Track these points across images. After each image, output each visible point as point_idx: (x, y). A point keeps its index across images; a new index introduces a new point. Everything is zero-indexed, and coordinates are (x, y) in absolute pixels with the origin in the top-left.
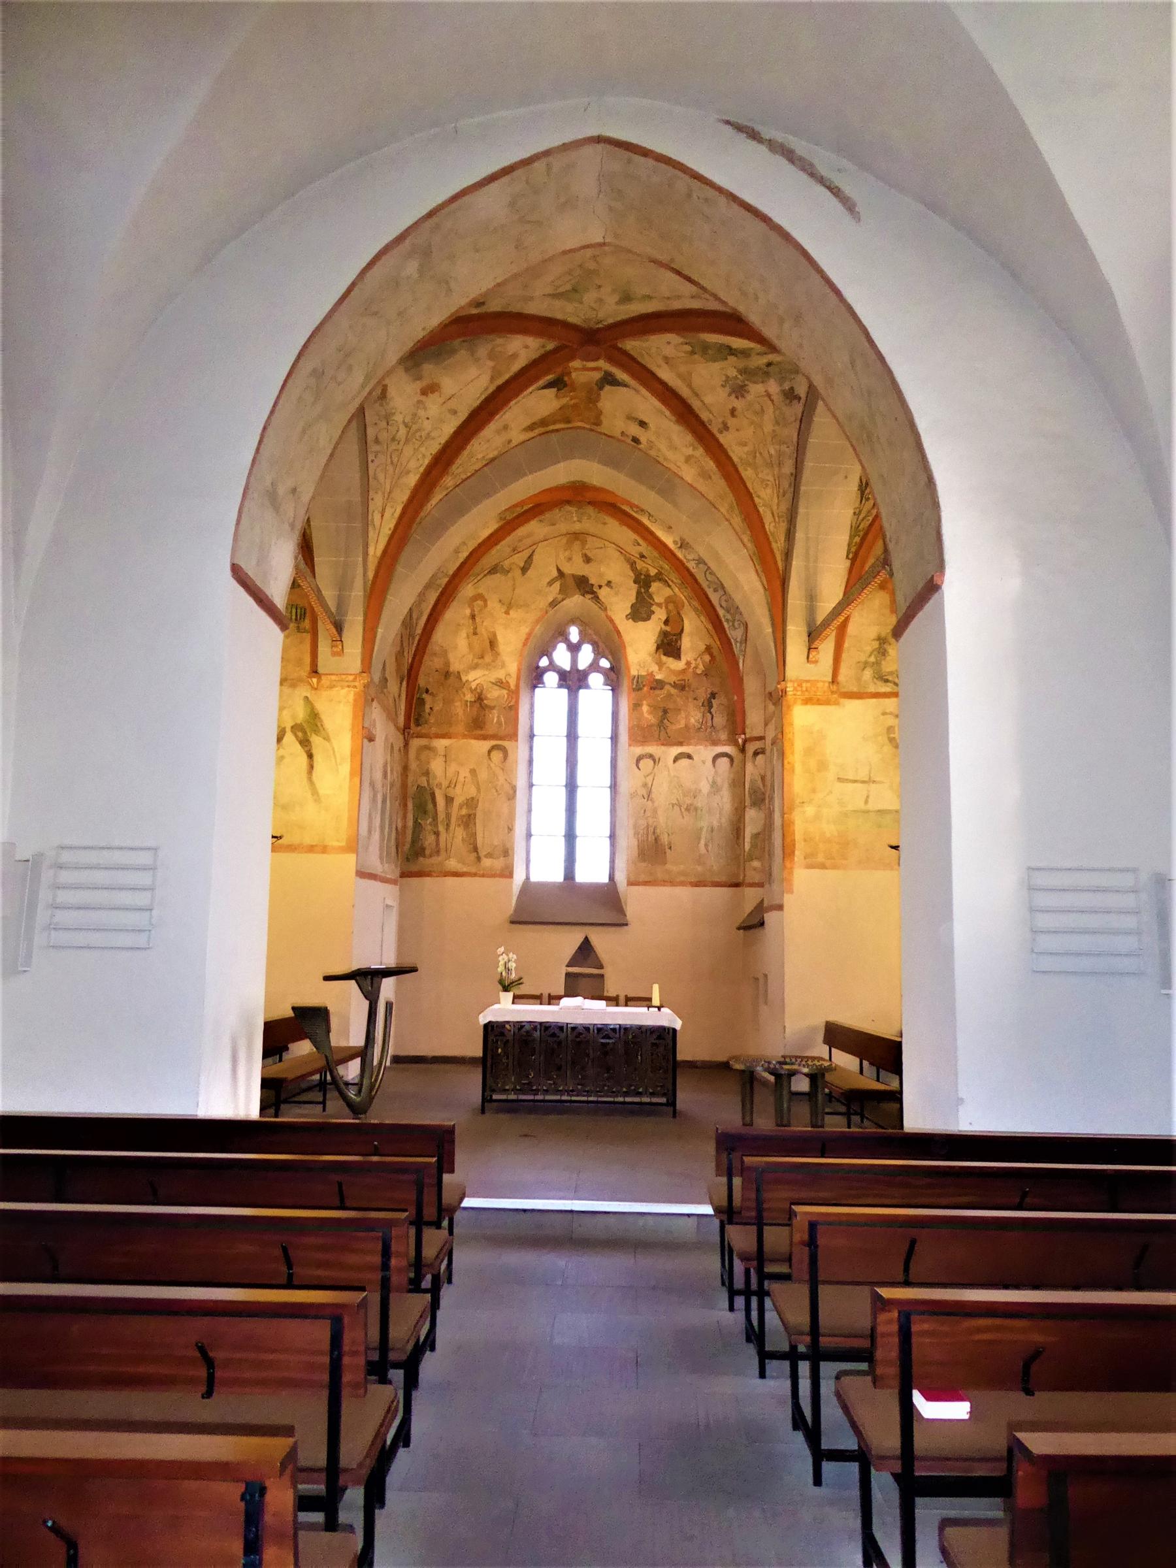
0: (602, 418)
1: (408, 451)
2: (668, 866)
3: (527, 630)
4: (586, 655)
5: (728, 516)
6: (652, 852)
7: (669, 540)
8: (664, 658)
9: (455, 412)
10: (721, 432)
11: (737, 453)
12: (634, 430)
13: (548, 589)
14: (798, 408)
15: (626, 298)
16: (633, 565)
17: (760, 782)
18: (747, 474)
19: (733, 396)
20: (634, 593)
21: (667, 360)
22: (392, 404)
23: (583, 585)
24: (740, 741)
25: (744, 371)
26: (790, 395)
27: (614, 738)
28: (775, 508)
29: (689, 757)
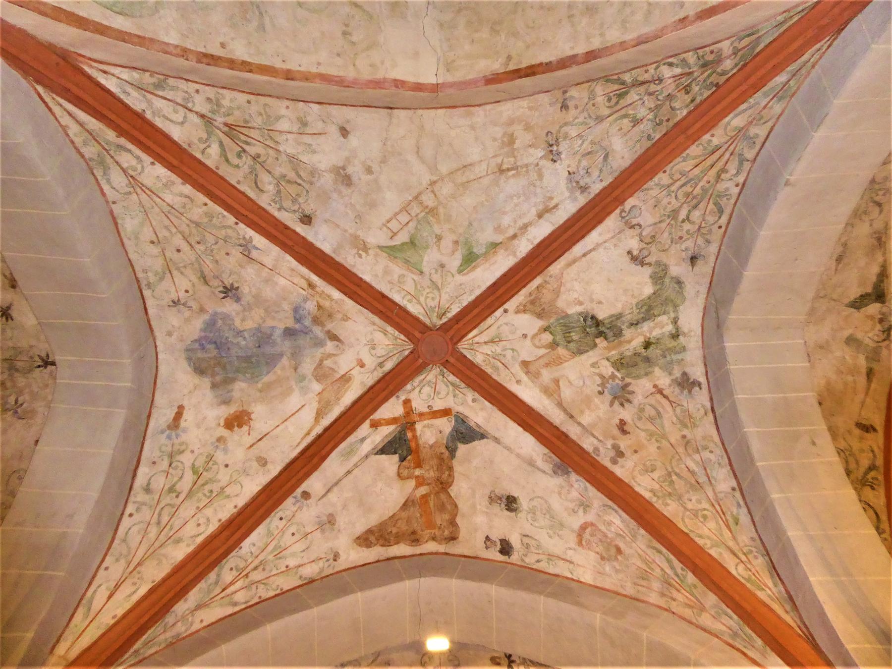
0: (458, 520)
1: (187, 511)
5: (662, 602)
9: (263, 462)
10: (614, 462)
12: (502, 525)
14: (702, 397)
15: (470, 260)
18: (670, 509)
19: (617, 403)
21: (525, 364)
22: (184, 437)
25: (619, 364)
26: (686, 383)
28: (731, 544)
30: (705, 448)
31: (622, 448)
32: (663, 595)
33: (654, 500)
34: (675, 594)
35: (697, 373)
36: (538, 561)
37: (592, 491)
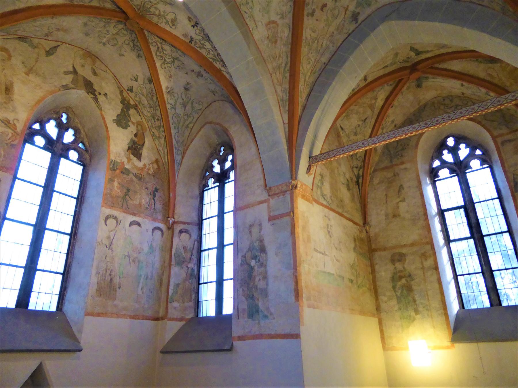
2: (116, 302)
3: (41, 94)
4: (69, 137)
5: (271, 71)
6: (108, 288)
7: (164, 84)
8: (132, 156)
10: (308, 16)
11: (307, 34)
13: (63, 76)
16: (121, 92)
17: (182, 249)
18: (304, 50)
20: (120, 108)
23: (89, 87)
24: (171, 222)
27: (80, 200)
28: (307, 78)
29: (139, 225)
30: (333, 44)
31: (315, 14)
32: (274, 69)
33: (304, 41)
34: (278, 73)
35: (361, 18)
36: (246, 12)
37: (291, 15)
